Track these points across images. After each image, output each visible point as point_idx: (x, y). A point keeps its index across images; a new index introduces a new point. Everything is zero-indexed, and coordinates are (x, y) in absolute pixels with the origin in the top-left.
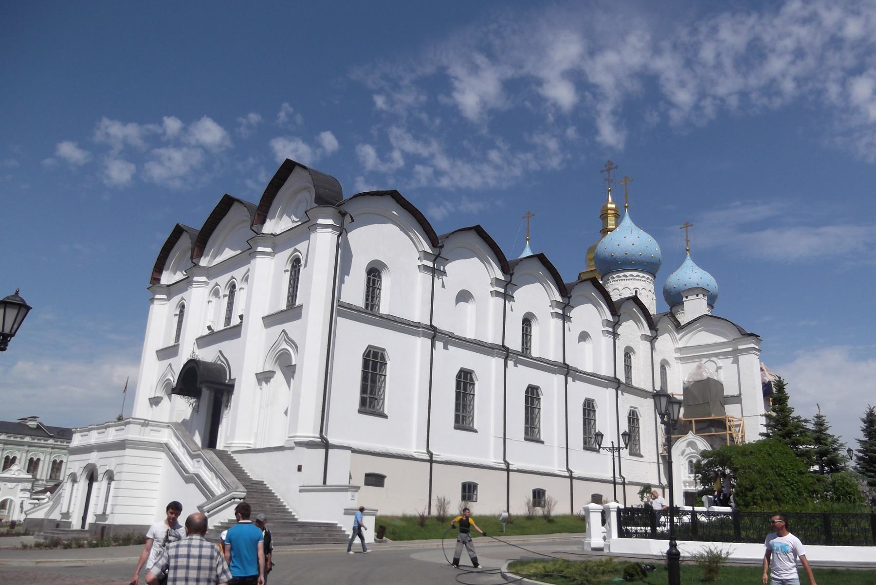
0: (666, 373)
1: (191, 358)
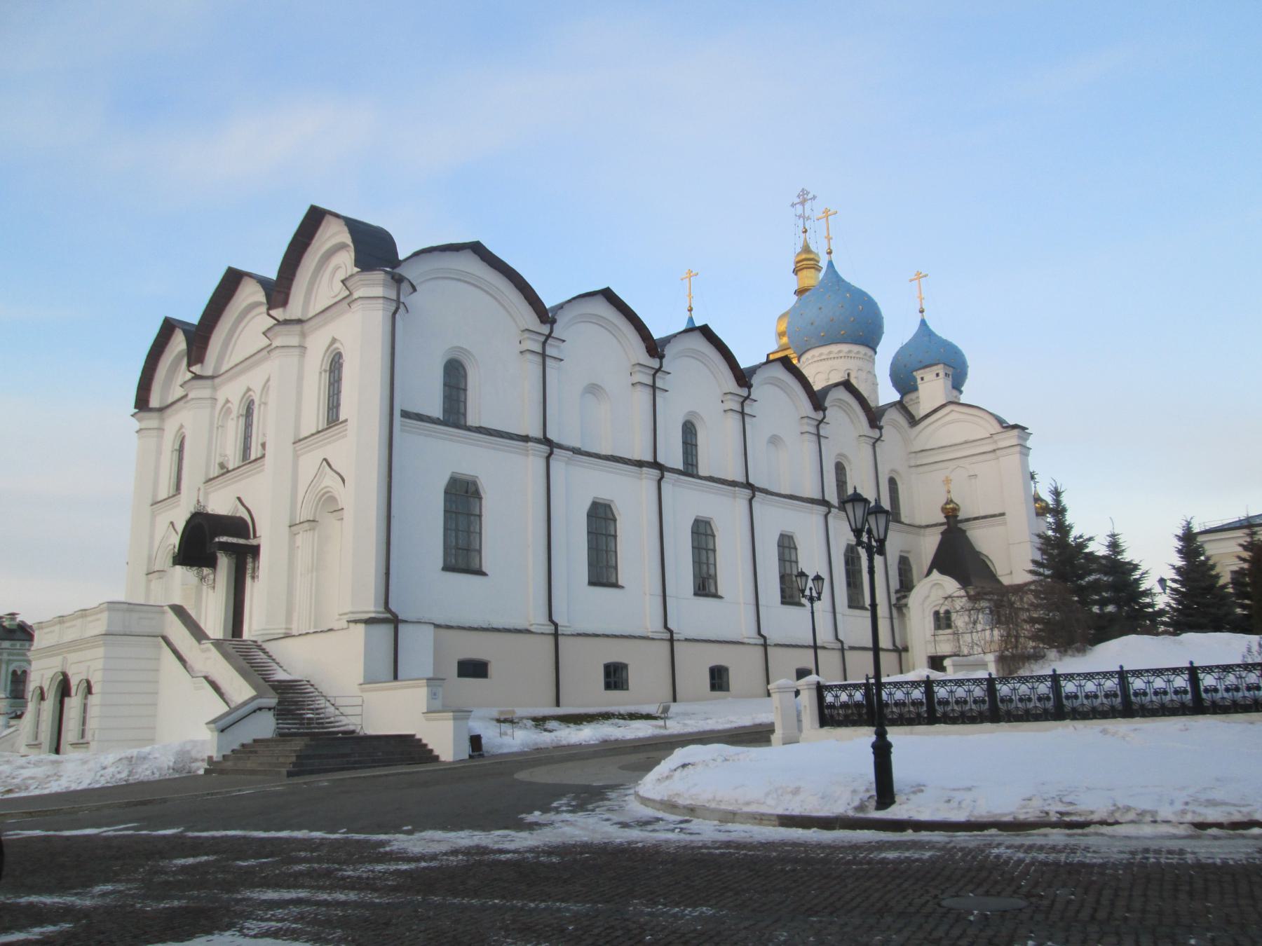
1: (196, 510)
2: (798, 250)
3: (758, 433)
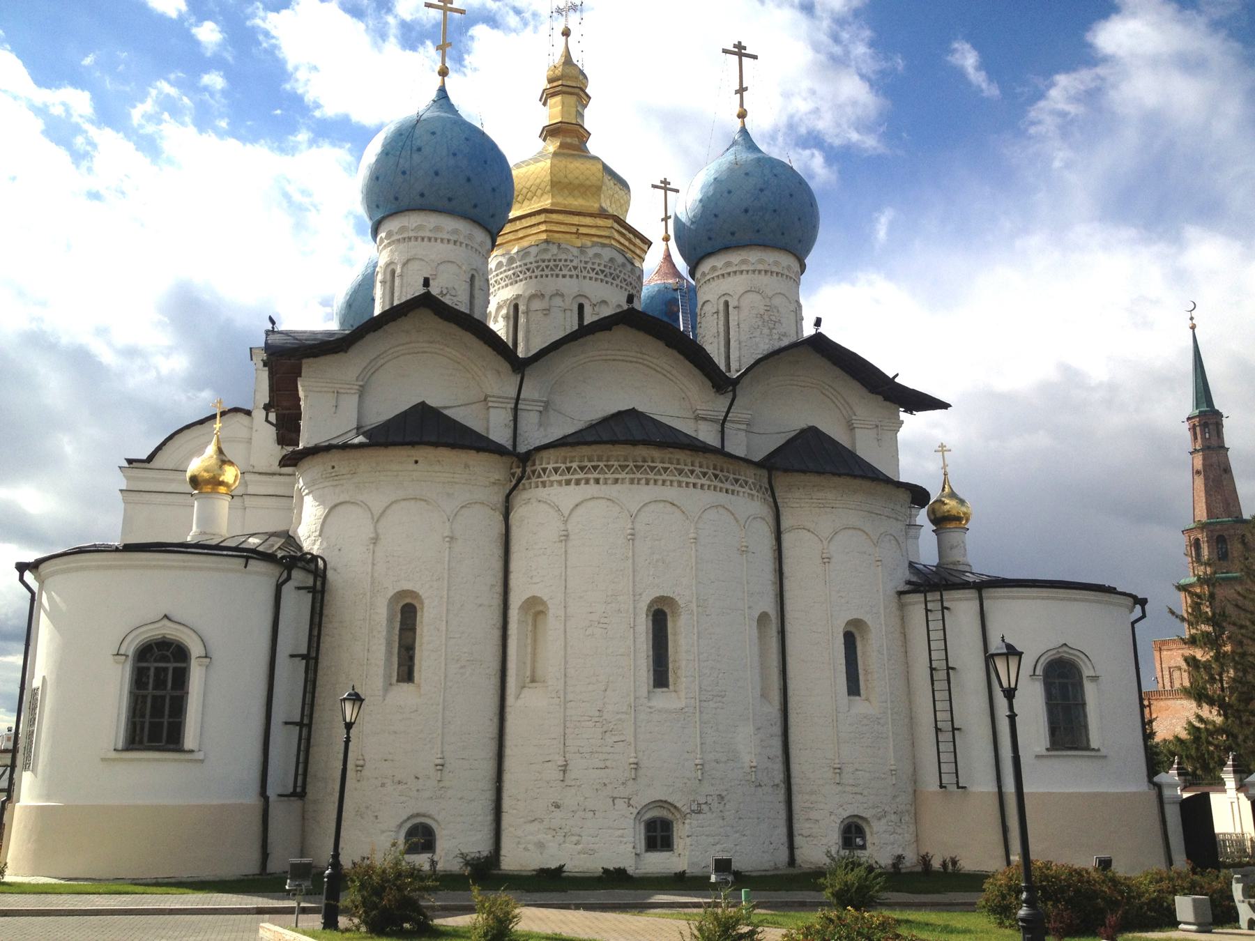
2: (558, 58)
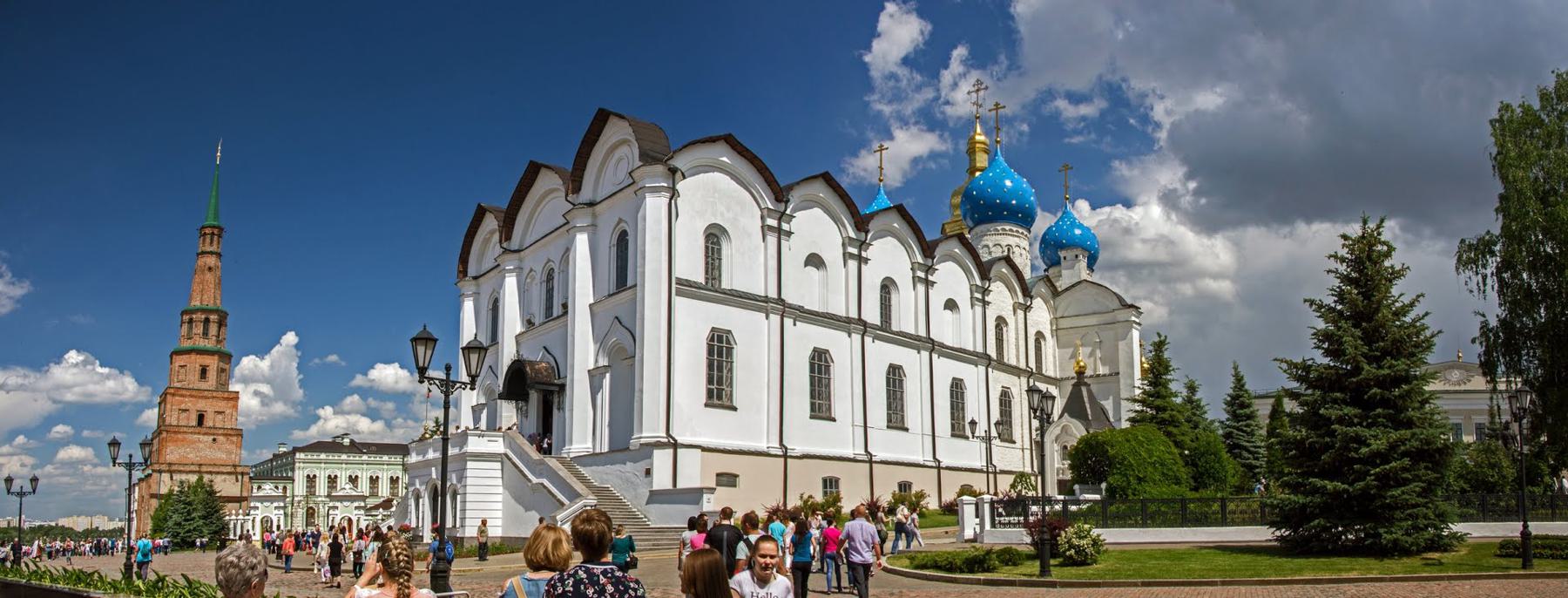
0: (1041, 348)
3: (938, 298)
